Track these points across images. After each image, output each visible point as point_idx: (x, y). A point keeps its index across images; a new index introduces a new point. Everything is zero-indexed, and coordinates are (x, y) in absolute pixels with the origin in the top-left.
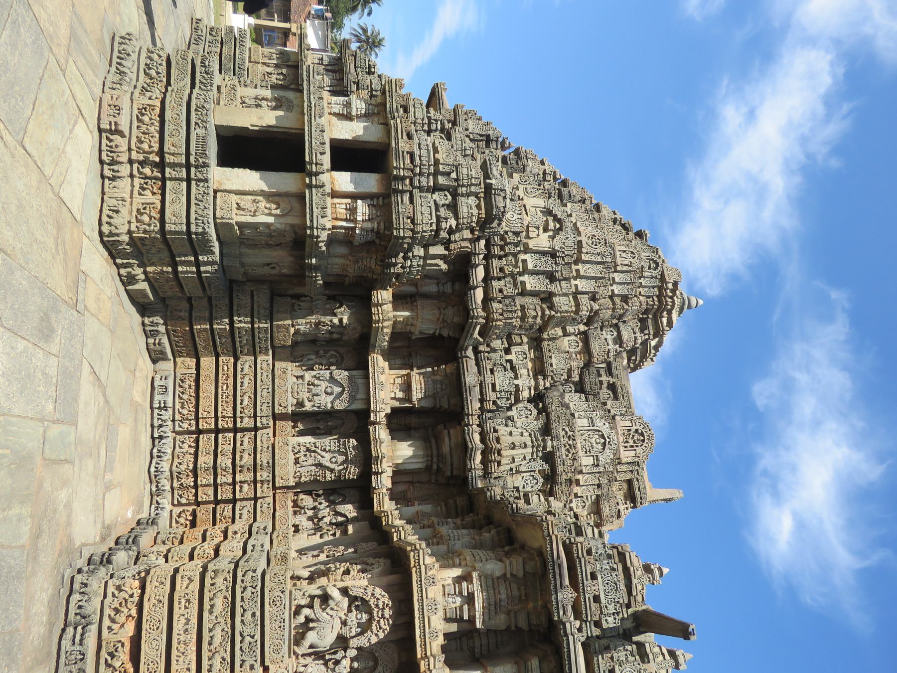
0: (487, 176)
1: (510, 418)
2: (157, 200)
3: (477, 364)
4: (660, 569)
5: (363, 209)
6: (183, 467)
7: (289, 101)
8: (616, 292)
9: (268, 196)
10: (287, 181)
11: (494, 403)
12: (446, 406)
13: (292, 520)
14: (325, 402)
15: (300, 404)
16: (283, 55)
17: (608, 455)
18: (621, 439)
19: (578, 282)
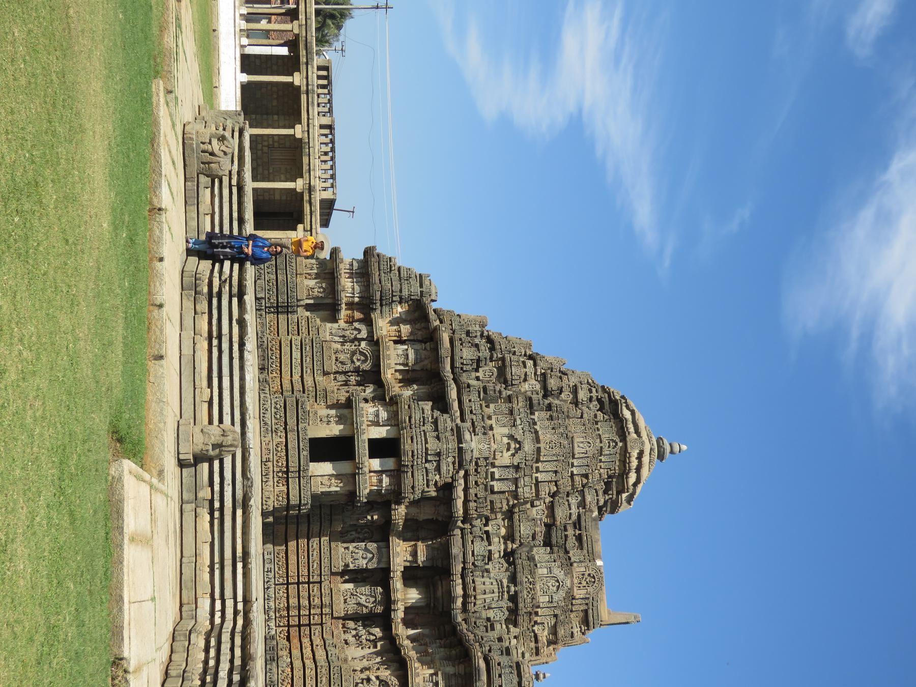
0: (460, 441)
1: (488, 571)
2: (284, 488)
3: (462, 538)
4: (544, 674)
5: (386, 480)
6: (282, 605)
7: (345, 416)
8: (575, 472)
9: (337, 476)
10: (345, 467)
11: (473, 564)
12: (440, 566)
13: (343, 636)
14: (363, 563)
15: (347, 565)
16: (322, 263)
17: (562, 593)
18: (576, 581)
19: (538, 475)
